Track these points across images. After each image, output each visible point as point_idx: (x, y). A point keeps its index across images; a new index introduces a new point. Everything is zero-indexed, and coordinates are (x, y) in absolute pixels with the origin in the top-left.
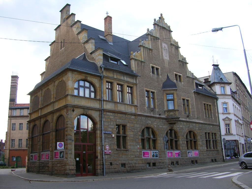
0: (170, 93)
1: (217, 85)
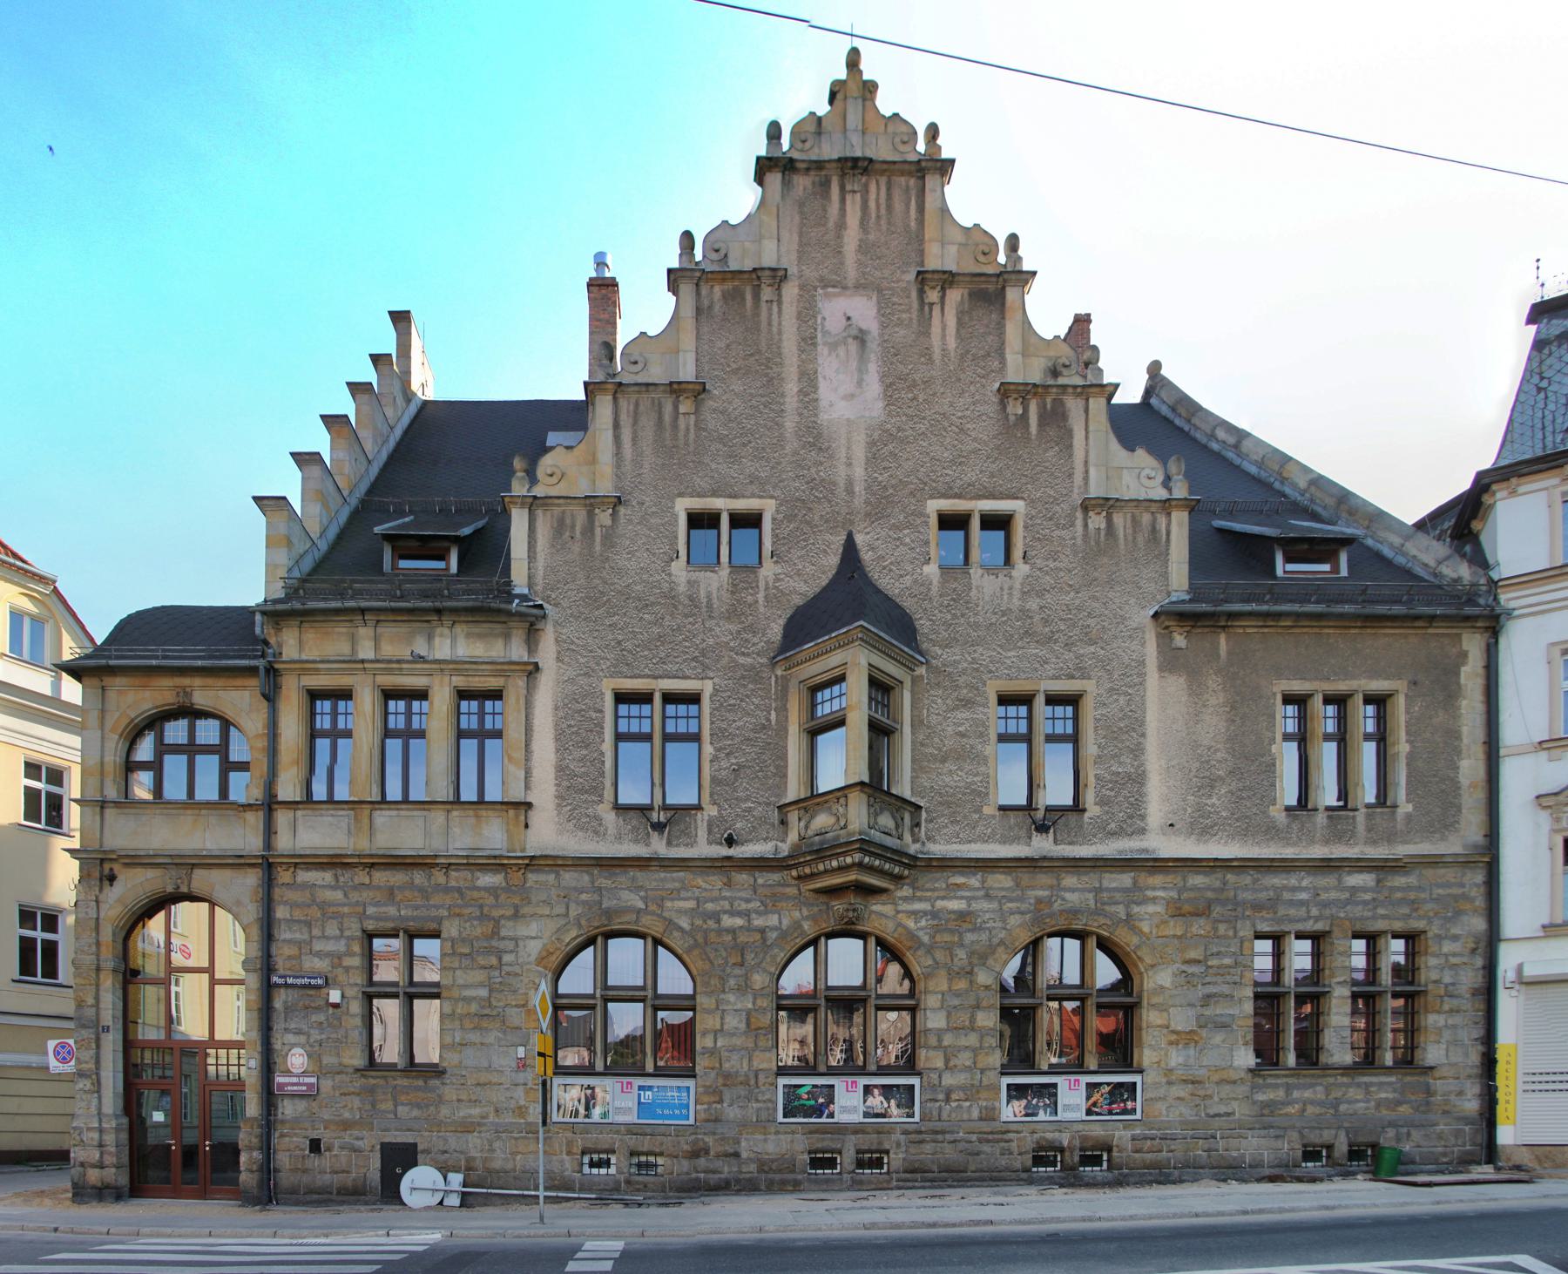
0: (825, 677)
1: (1513, 493)
